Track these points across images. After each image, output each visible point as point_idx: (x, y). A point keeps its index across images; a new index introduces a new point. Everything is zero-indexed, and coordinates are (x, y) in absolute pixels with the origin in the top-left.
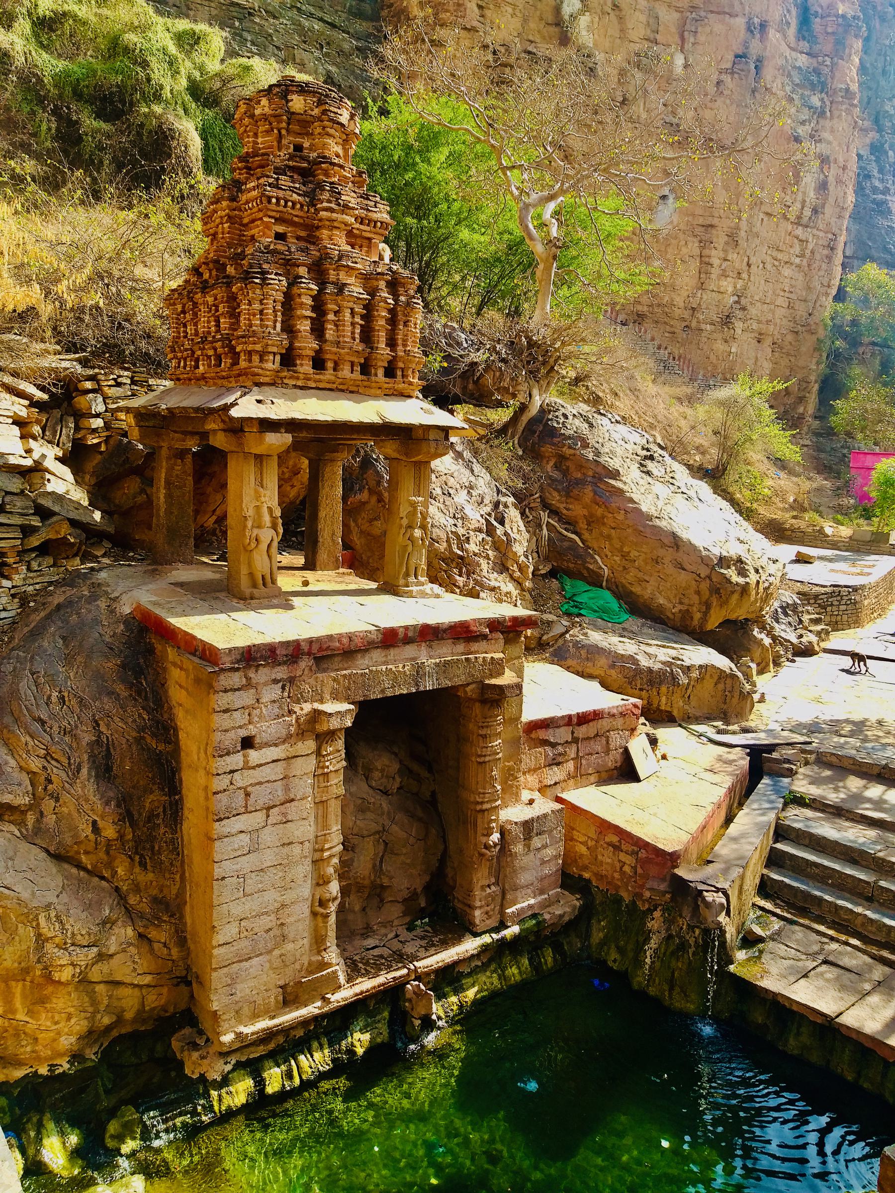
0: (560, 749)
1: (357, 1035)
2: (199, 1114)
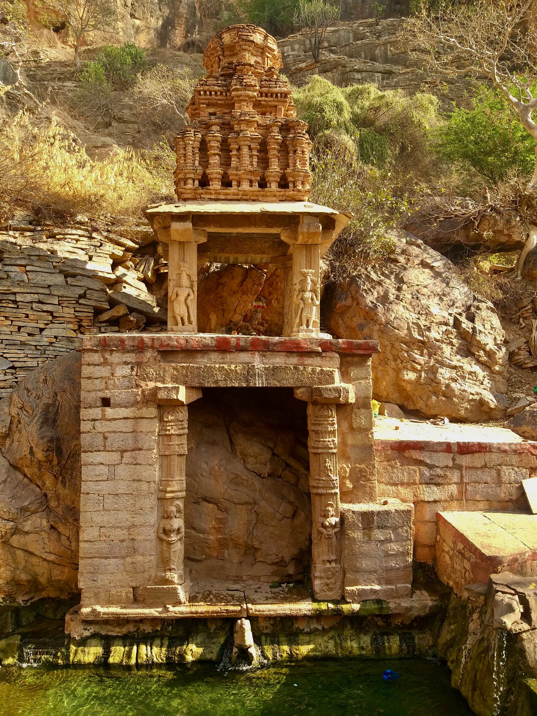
0: (439, 471)
1: (193, 647)
2: (58, 658)
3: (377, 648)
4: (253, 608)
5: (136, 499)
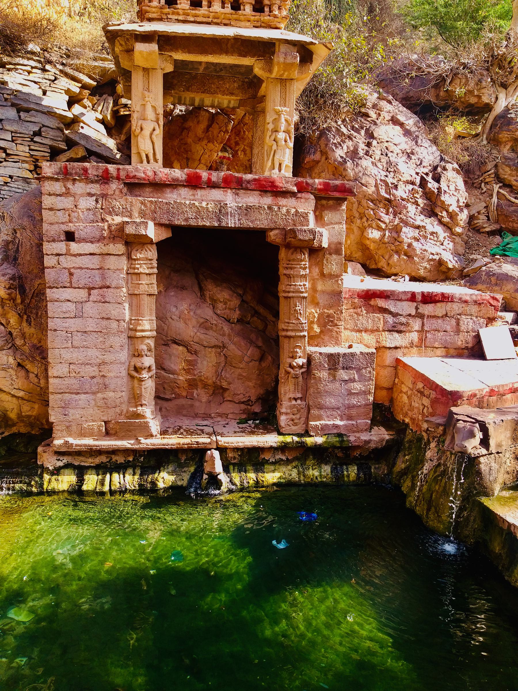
0: (403, 320)
3: (337, 476)
4: (223, 441)
5: (106, 336)
